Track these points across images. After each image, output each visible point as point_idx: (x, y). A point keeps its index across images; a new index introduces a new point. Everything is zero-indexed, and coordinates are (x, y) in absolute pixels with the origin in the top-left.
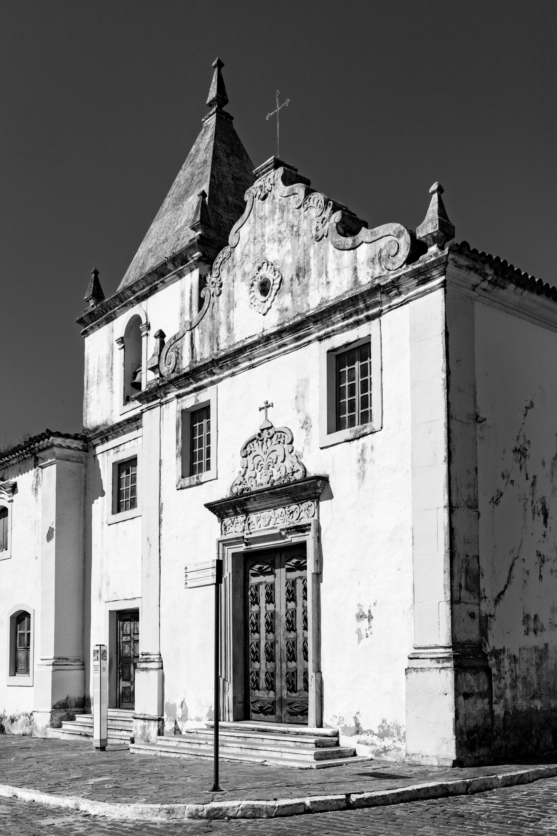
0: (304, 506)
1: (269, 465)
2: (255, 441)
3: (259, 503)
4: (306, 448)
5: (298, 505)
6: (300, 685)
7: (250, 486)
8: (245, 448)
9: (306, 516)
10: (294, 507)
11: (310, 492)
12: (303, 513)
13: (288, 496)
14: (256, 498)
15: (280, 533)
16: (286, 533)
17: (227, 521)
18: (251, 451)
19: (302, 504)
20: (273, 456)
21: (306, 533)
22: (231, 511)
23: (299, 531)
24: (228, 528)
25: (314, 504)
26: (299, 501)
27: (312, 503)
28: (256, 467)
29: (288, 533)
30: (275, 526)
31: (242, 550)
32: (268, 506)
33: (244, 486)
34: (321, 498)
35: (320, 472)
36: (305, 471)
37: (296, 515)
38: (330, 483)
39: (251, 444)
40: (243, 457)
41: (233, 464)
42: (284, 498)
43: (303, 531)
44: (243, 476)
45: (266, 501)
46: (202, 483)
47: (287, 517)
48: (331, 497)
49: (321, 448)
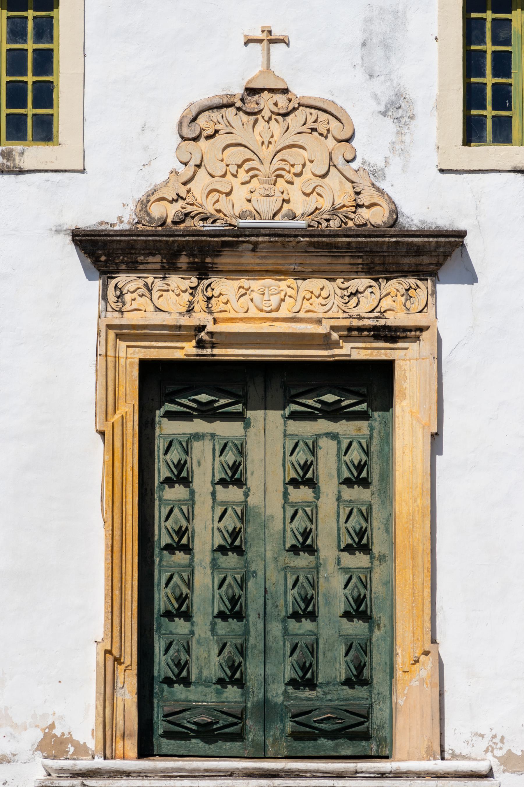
0: (396, 285)
1: (281, 176)
2: (232, 110)
3: (264, 257)
4: (396, 162)
5: (376, 280)
6: (333, 666)
7: (214, 212)
8: (194, 120)
9: (397, 306)
10: (361, 283)
11: (426, 260)
12: (389, 300)
13: (359, 257)
14: (261, 246)
15: (327, 336)
16: (340, 337)
17: (127, 280)
18: (217, 131)
19: (388, 279)
20: (295, 157)
21: (400, 345)
22: (158, 259)
23: (387, 339)
24: (128, 297)
25: (424, 287)
26: (379, 272)
27: (419, 283)
28: (233, 169)
29: (347, 338)
30: (300, 315)
31: (179, 355)
32: (283, 268)
33: (189, 209)
34: (441, 274)
35: (442, 219)
36: (395, 212)
37: (367, 302)
38: (468, 249)
39: (215, 115)
40: (184, 139)
41: (146, 149)
42: (347, 260)
43: (394, 339)
44: (185, 184)
45: (284, 257)
46: (21, 172)
47: (338, 301)
48: (470, 277)
49: (442, 171)
